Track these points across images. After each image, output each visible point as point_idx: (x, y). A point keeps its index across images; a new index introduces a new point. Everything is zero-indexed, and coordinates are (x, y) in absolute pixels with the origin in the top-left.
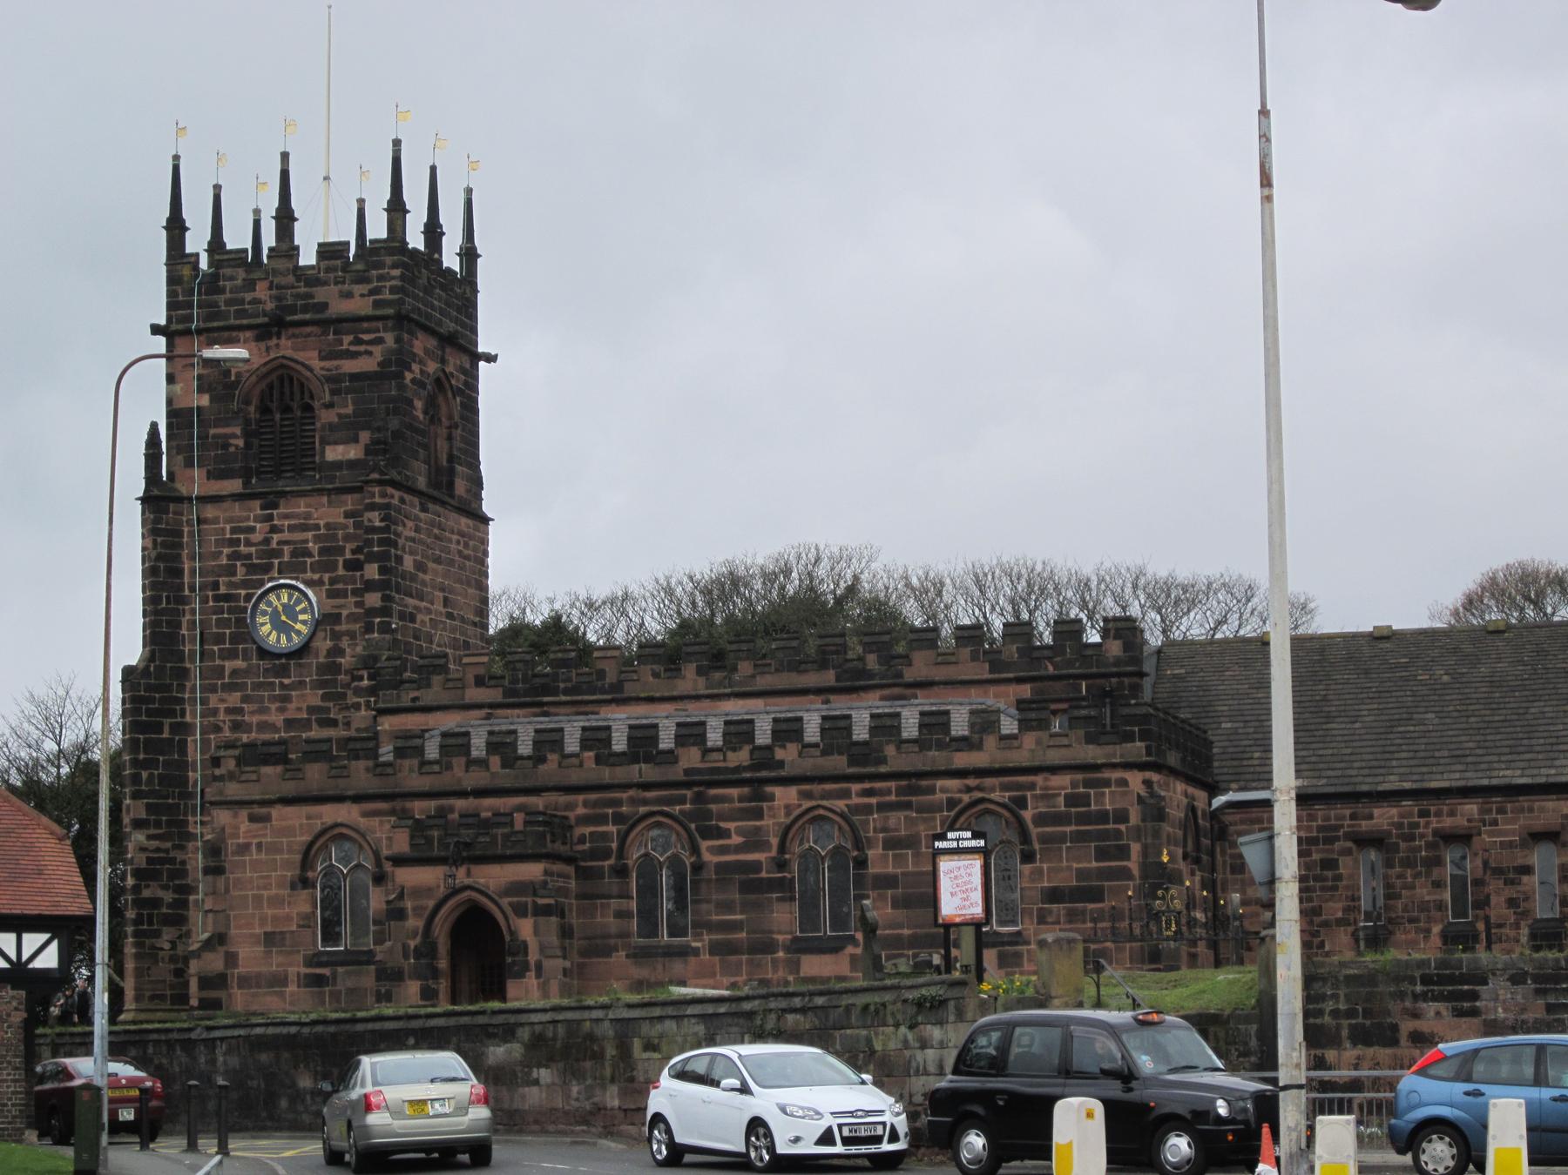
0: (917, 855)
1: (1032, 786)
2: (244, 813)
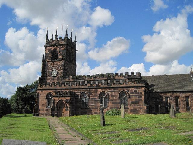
0: (115, 97)
2: (40, 91)
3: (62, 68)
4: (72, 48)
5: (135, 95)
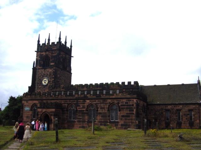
1: (120, 101)
2: (26, 101)
3: (53, 76)
4: (66, 54)
5: (127, 108)
